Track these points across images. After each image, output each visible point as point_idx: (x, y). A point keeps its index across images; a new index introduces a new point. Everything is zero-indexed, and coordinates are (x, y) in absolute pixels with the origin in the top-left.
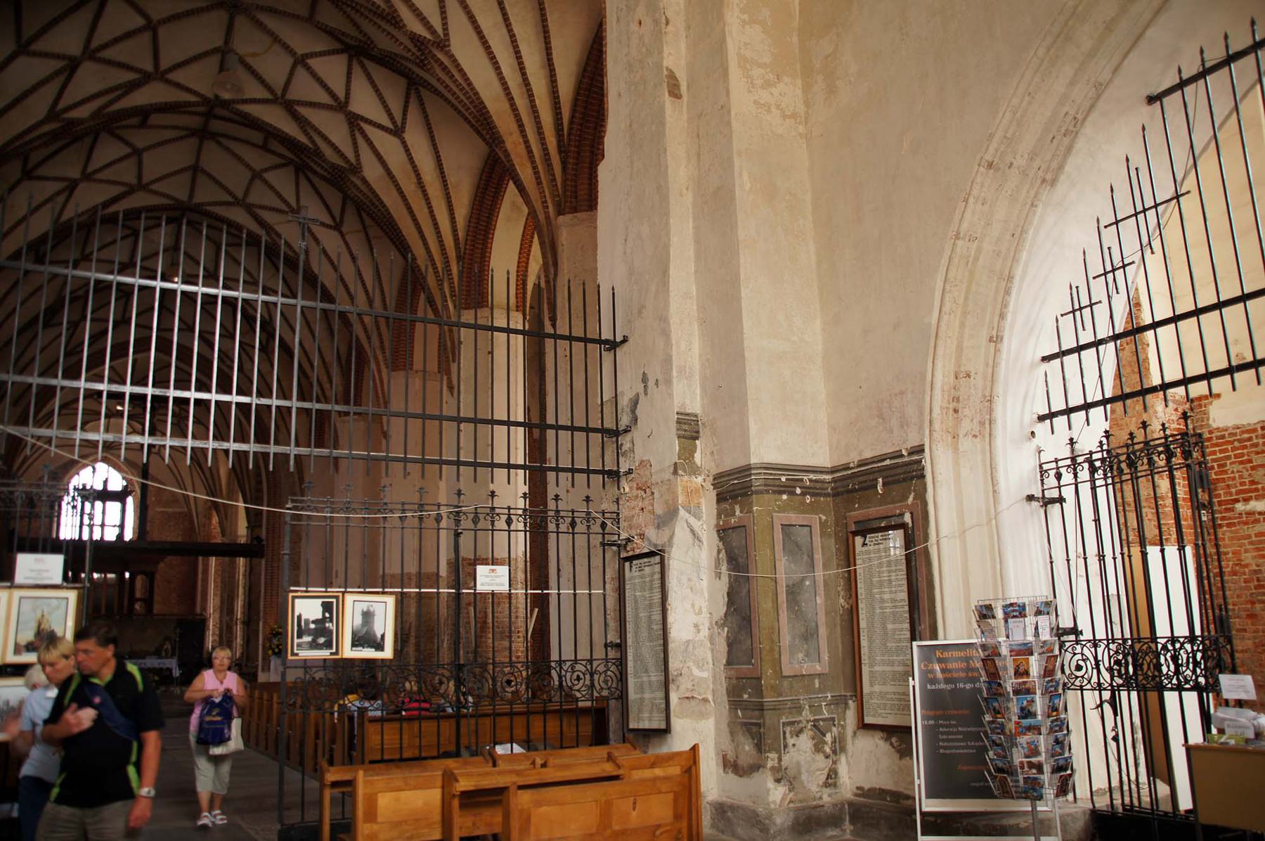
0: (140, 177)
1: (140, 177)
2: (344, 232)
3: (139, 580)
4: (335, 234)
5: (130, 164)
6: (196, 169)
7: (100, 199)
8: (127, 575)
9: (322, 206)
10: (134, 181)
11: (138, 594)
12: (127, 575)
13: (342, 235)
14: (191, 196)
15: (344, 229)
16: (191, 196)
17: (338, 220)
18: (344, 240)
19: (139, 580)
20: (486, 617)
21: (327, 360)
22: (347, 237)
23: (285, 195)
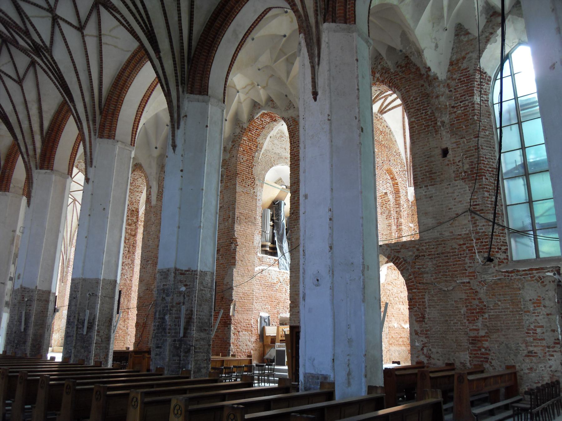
2: (85, 33)
13: (83, 36)
15: (85, 32)
18: (83, 39)
21: (33, 129)
22: (87, 39)
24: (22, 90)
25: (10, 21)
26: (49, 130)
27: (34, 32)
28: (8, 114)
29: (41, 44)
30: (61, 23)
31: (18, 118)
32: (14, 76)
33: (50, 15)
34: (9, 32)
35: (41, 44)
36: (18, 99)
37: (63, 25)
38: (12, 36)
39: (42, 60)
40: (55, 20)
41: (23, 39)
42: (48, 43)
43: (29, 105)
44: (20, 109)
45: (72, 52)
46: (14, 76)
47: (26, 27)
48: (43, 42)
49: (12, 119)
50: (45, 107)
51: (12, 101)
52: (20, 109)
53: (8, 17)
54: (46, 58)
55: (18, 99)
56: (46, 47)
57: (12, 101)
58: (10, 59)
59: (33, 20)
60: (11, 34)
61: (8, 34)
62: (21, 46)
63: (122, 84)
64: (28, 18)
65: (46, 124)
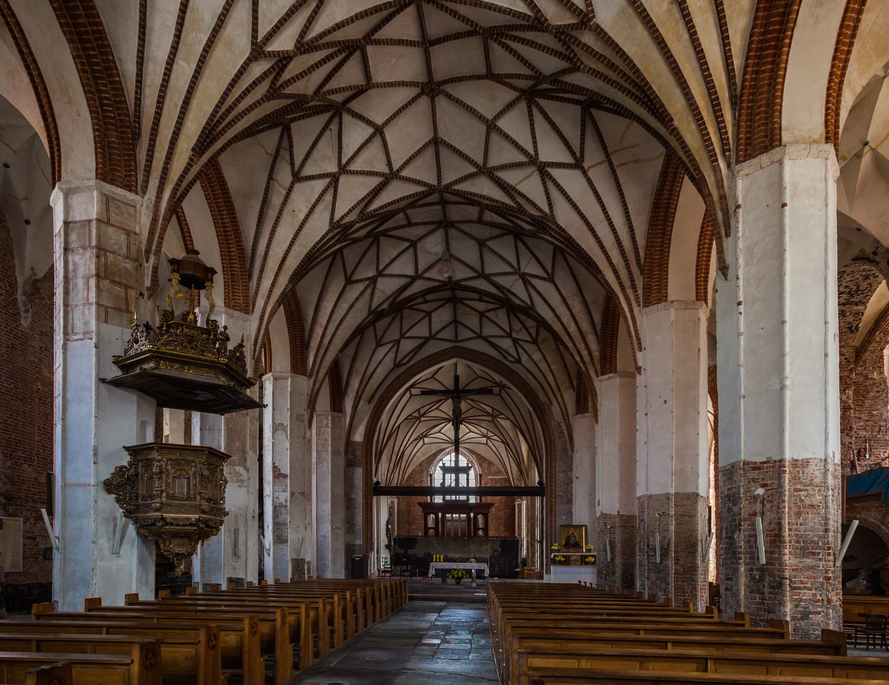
0: (389, 164)
1: (389, 164)
3: (480, 517)
4: (577, 173)
5: (375, 147)
6: (436, 142)
7: (362, 193)
8: (472, 515)
9: (561, 145)
10: (383, 168)
11: (481, 526)
12: (472, 515)
14: (439, 178)
16: (439, 178)
17: (578, 155)
19: (480, 517)
20: (780, 529)
23: (522, 143)
24: (556, 286)
25: (494, 204)
26: (602, 324)
27: (527, 203)
28: (551, 323)
29: (540, 214)
30: (550, 170)
31: (561, 323)
32: (543, 274)
33: (534, 168)
34: (508, 220)
35: (540, 214)
36: (555, 299)
37: (555, 173)
38: (514, 223)
39: (550, 235)
40: (543, 170)
41: (522, 220)
42: (546, 209)
43: (570, 302)
44: (562, 311)
45: (578, 204)
46: (543, 274)
47: (516, 202)
48: (539, 209)
49: (557, 327)
50: (589, 299)
51: (549, 306)
52: (562, 311)
53: (494, 200)
54: (553, 230)
55: (555, 299)
56: (547, 214)
57: (549, 306)
58: (531, 256)
59: (520, 188)
60: (511, 221)
61: (511, 224)
62: (527, 230)
63: (663, 214)
64: (514, 189)
65: (597, 318)
